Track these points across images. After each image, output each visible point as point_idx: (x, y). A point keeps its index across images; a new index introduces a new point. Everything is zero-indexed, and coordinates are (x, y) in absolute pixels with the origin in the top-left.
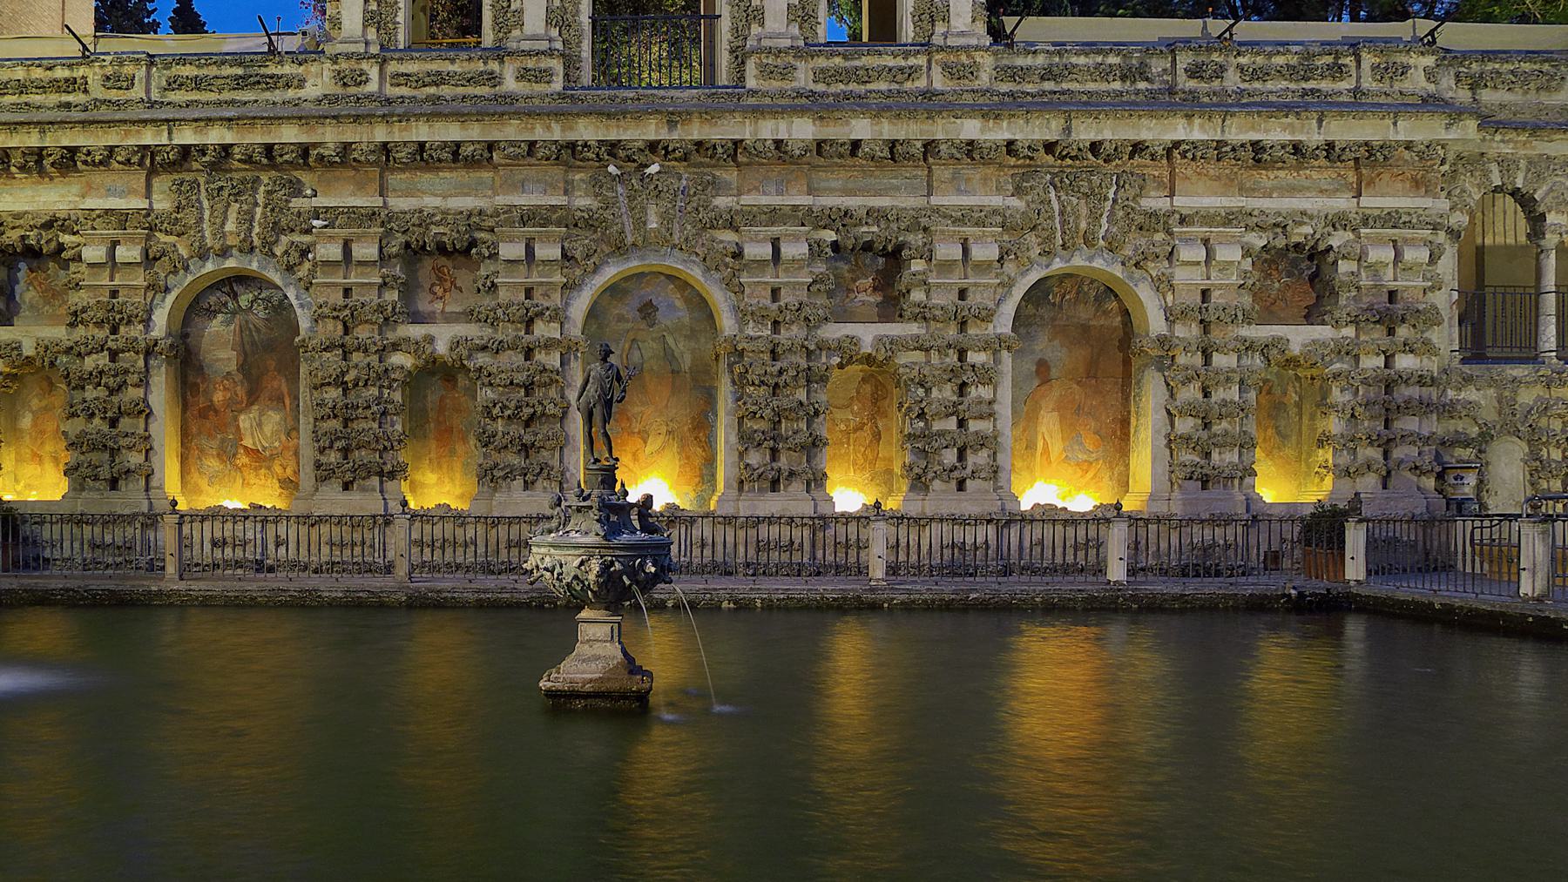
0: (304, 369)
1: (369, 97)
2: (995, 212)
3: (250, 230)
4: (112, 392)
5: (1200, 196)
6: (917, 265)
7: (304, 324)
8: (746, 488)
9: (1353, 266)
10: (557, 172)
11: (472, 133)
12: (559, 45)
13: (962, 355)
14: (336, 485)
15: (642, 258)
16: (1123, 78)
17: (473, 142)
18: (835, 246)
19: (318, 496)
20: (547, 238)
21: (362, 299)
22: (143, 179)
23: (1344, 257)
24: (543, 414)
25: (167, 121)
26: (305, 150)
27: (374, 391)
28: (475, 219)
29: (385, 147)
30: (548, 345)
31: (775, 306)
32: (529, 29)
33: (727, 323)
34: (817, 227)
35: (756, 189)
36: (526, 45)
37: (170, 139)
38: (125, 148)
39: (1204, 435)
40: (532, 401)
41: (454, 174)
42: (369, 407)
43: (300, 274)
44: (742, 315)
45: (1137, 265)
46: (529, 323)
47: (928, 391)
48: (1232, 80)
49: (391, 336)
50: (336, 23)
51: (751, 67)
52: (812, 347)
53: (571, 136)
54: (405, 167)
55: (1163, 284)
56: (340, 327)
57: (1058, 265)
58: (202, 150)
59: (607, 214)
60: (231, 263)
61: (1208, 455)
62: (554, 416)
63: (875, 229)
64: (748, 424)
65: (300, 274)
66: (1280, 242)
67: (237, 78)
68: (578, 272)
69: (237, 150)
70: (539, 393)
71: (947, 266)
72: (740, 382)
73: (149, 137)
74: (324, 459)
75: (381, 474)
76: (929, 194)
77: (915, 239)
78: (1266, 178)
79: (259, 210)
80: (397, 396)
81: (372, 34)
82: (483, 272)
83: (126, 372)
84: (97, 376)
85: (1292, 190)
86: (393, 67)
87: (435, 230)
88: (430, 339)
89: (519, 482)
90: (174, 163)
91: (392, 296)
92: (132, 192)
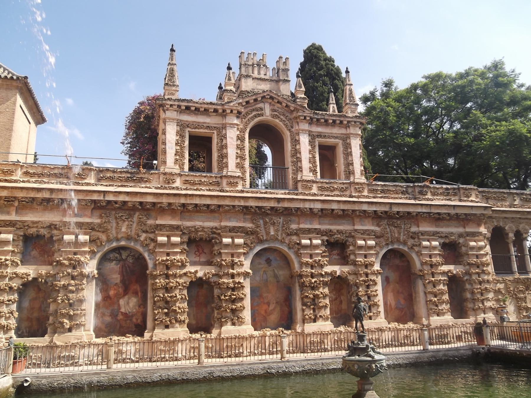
0: (150, 282)
1: (177, 188)
2: (372, 231)
3: (131, 231)
4: (73, 292)
5: (425, 227)
6: (351, 248)
7: (150, 264)
8: (306, 322)
9: (466, 248)
10: (241, 216)
11: (215, 202)
12: (240, 174)
13: (367, 275)
14: (163, 327)
15: (269, 244)
16: (403, 193)
17: (214, 205)
18: (327, 241)
19: (156, 331)
20: (239, 237)
21: (173, 258)
22: (90, 211)
23: (464, 246)
25: (104, 192)
26: (154, 204)
28: (214, 230)
29: (184, 205)
30: (239, 274)
31: (311, 261)
32: (230, 170)
33: (296, 265)
34: (322, 235)
35: (304, 223)
36: (229, 174)
37: (104, 197)
38: (85, 200)
39: (436, 299)
41: (206, 214)
42: (176, 296)
43: (151, 247)
44: (301, 264)
45: (412, 248)
46: (233, 265)
47: (358, 288)
48: (429, 196)
49: (184, 271)
50: (165, 162)
51: (300, 185)
52: (323, 273)
53: (247, 204)
54: (189, 211)
55: (419, 254)
56: (165, 267)
57: (390, 247)
58: (116, 202)
59: (258, 230)
60: (123, 243)
61: (437, 306)
63: (339, 236)
64: (306, 300)
65: (150, 248)
66: (447, 241)
67: (128, 177)
68: (249, 249)
69: (129, 203)
71: (361, 247)
72: (302, 286)
73: (95, 197)
76: (354, 225)
77: (350, 240)
78: (441, 224)
79: (135, 225)
80: (185, 292)
81: (177, 167)
82: (216, 248)
84: (65, 287)
85: (448, 226)
86: (184, 178)
87: (200, 233)
88: (196, 272)
89: (229, 323)
90: (103, 206)
91: (183, 257)
92: (85, 216)
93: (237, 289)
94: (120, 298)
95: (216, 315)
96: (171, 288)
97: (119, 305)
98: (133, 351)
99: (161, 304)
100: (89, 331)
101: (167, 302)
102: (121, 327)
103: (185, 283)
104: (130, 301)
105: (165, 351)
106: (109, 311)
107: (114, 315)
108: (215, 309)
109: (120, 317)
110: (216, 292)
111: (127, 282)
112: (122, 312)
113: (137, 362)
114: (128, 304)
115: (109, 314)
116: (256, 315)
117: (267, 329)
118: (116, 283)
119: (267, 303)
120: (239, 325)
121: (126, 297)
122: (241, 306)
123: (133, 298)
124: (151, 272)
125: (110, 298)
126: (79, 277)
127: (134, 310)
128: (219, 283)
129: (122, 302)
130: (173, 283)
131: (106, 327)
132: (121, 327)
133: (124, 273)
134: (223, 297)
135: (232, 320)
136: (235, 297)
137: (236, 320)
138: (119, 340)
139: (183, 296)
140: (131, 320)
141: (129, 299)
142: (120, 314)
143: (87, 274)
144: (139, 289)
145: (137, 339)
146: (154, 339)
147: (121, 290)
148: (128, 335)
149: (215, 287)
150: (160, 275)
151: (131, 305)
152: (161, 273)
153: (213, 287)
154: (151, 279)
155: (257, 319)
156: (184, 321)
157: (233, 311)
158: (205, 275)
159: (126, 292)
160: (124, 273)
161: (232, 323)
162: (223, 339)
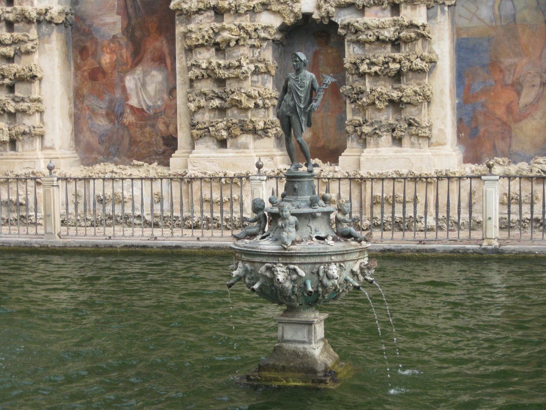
0: (180, 29)
14: (212, 144)
24: (411, 70)
27: (245, 50)
40: (397, 55)
42: (240, 66)
62: (421, 71)
70: (405, 50)
74: (198, 117)
75: (254, 132)
80: (268, 54)
83: (20, 41)
89: (386, 138)
93: (406, 43)
94: (126, 72)
95: (349, 116)
96: (228, 45)
97: (124, 89)
98: (147, 201)
99: (206, 86)
100: (51, 148)
101: (221, 82)
102: (133, 142)
103: (265, 28)
104: (148, 79)
105: (211, 202)
106: (104, 105)
107: (114, 114)
108: (348, 101)
109: (129, 118)
110: (351, 53)
111: (138, 34)
112: (132, 107)
113: (156, 225)
114: (142, 87)
115: (104, 112)
116: (481, 118)
117: (500, 160)
118: (114, 37)
119: (512, 85)
120: (412, 145)
121: (139, 70)
122: (416, 92)
123: (154, 73)
124: (179, 4)
125: (104, 73)
126: (21, 25)
127: (159, 103)
128: (357, 31)
129: (130, 82)
130: (230, 30)
131: (101, 142)
132: (133, 142)
133: (131, 11)
134: (364, 68)
135: (393, 130)
136: (398, 66)
137: (407, 130)
138: (112, 172)
139: (260, 65)
140: (153, 126)
141: (145, 73)
142: (128, 110)
143: (34, 15)
144: (166, 50)
145: (154, 169)
146: (191, 172)
147: (126, 53)
148: (135, 162)
149: (348, 38)
150: (199, 11)
151: (151, 88)
152: (201, 5)
153: (343, 38)
154: (181, 23)
155: (482, 129)
156: (265, 131)
157: (396, 105)
158: (319, 7)
159: (137, 56)
160: (131, 11)
161: (394, 139)
162: (363, 179)
